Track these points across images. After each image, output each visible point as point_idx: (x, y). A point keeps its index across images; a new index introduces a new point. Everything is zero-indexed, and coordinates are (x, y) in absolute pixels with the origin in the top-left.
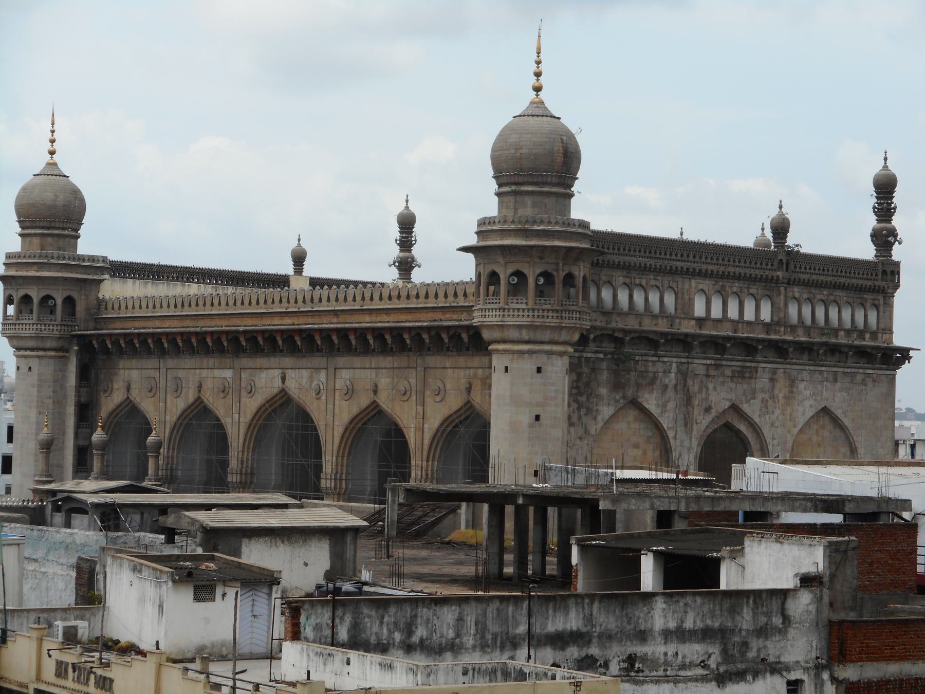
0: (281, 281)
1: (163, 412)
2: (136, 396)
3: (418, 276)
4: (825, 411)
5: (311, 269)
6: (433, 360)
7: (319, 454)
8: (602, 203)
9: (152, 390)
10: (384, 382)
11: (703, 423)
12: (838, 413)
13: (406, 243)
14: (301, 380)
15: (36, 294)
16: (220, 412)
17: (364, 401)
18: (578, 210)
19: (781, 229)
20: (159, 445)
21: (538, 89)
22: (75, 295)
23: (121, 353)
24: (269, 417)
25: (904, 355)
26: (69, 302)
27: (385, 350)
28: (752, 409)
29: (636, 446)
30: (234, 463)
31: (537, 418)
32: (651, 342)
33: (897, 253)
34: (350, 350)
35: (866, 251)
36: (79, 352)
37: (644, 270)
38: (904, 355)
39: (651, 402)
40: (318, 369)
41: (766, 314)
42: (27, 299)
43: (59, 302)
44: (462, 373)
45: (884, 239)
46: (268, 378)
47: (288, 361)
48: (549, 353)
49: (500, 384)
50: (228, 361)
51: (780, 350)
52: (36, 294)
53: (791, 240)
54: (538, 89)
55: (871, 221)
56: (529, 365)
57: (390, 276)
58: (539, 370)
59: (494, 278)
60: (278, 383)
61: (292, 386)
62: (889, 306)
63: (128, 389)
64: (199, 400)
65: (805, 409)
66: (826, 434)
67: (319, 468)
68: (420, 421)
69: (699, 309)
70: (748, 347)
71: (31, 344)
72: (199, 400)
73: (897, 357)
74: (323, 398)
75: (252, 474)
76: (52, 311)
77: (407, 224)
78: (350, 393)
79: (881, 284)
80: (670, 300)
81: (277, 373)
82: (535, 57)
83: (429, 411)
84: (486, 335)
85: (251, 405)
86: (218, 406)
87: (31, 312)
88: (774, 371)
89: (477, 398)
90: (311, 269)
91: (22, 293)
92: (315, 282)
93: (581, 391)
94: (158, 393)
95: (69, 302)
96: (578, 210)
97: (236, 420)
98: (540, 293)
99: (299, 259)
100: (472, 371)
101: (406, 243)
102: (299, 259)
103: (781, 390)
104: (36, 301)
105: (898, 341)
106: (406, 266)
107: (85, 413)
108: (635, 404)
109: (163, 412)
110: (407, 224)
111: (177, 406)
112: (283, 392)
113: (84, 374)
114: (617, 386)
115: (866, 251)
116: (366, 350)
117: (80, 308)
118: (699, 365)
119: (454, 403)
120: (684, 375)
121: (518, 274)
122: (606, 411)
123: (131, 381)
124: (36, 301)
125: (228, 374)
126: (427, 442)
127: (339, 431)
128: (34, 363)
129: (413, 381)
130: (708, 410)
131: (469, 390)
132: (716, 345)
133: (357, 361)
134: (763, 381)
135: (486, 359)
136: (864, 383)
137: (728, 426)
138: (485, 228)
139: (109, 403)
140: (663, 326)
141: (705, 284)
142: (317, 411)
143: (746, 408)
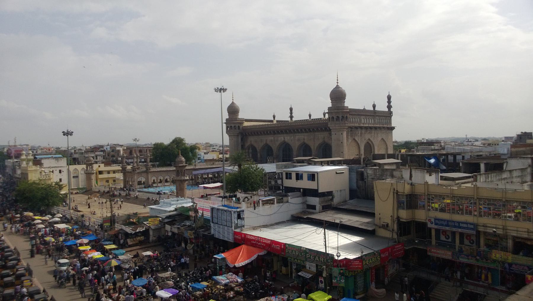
0: (272, 121)
1: (259, 146)
2: (252, 143)
3: (294, 119)
4: (382, 139)
5: (276, 119)
6: (317, 133)
8: (350, 103)
10: (306, 138)
11: (365, 142)
13: (291, 113)
14: (287, 138)
15: (233, 126)
16: (271, 145)
18: (346, 105)
19: (374, 106)
21: (338, 83)
25: (393, 128)
27: (306, 132)
28: (372, 139)
30: (274, 154)
32: (356, 128)
33: (392, 110)
34: (299, 132)
35: (387, 110)
37: (355, 115)
38: (393, 128)
39: (357, 139)
42: (231, 126)
45: (389, 107)
46: (281, 138)
47: (285, 135)
49: (334, 137)
51: (376, 128)
52: (233, 126)
53: (377, 109)
54: (338, 83)
55: (387, 104)
57: (289, 119)
59: (333, 118)
60: (283, 139)
61: (286, 140)
62: (391, 119)
65: (380, 138)
68: (314, 144)
69: (363, 122)
70: (371, 128)
73: (393, 128)
77: (291, 109)
84: (331, 128)
85: (278, 143)
90: (276, 119)
92: (277, 121)
94: (258, 142)
95: (239, 127)
96: (346, 105)
97: (275, 147)
99: (274, 117)
101: (291, 113)
102: (274, 117)
105: (393, 126)
106: (291, 117)
107: (243, 147)
108: (354, 139)
109: (259, 146)
110: (291, 109)
111: (261, 145)
112: (284, 141)
113: (242, 139)
114: (351, 136)
116: (302, 132)
118: (363, 131)
119: (321, 141)
120: (361, 133)
121: (338, 117)
122: (350, 141)
123: (251, 140)
125: (272, 138)
127: (297, 147)
132: (366, 128)
133: (300, 134)
134: (373, 134)
135: (328, 133)
138: (329, 109)
139: (247, 144)
140: (357, 125)
141: (364, 117)
142: (291, 143)
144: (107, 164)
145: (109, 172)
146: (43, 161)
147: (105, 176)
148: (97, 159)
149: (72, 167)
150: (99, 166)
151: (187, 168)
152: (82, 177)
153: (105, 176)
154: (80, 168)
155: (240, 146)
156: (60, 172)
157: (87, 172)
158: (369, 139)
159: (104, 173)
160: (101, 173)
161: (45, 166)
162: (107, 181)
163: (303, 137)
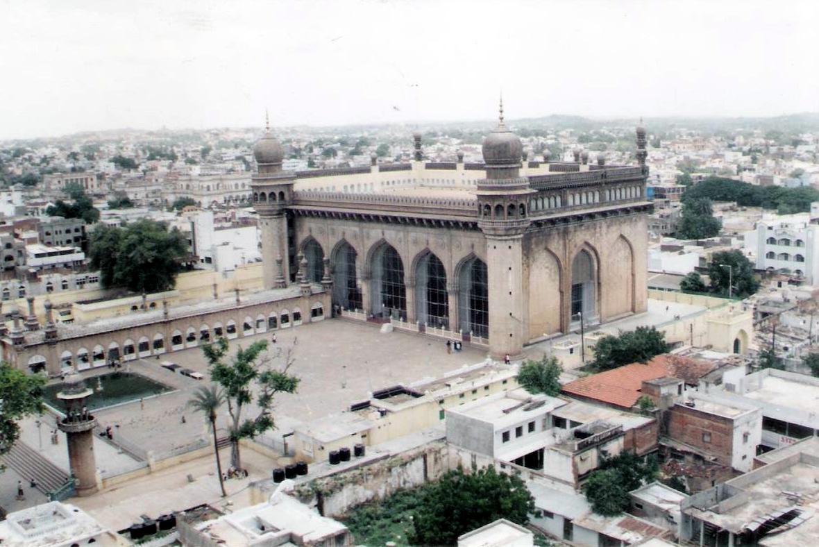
1: (328, 245)
4: (622, 237)
7: (401, 268)
9: (322, 232)
10: (432, 240)
12: (626, 236)
14: (392, 235)
15: (267, 193)
17: (423, 247)
20: (328, 261)
22: (283, 191)
23: (306, 216)
24: (377, 249)
26: (282, 194)
29: (547, 268)
31: (510, 269)
36: (287, 216)
40: (399, 231)
41: (597, 200)
42: (263, 194)
43: (277, 195)
44: (469, 239)
45: (642, 157)
46: (376, 233)
47: (385, 226)
48: (514, 240)
50: (357, 223)
52: (267, 193)
56: (505, 245)
58: (510, 247)
63: (310, 231)
64: (344, 239)
66: (620, 245)
67: (402, 275)
68: (451, 259)
71: (267, 213)
72: (344, 239)
74: (403, 243)
75: (371, 273)
76: (274, 199)
78: (415, 242)
79: (642, 176)
80: (558, 199)
81: (380, 231)
82: (499, 103)
83: (454, 256)
85: (369, 244)
86: (353, 243)
87: (265, 199)
88: (601, 224)
89: (478, 253)
91: (261, 192)
93: (527, 251)
94: (328, 236)
95: (282, 194)
98: (509, 214)
100: (473, 239)
103: (604, 229)
104: (267, 195)
107: (292, 240)
112: (383, 239)
115: (634, 164)
117: (287, 197)
124: (267, 195)
125: (357, 229)
126: (453, 269)
127: (411, 259)
128: (268, 221)
129: (445, 241)
130: (575, 246)
131: (473, 246)
136: (636, 221)
137: (583, 250)
139: (302, 237)
143: (592, 242)
155: (286, 240)
158: (587, 243)
163: (425, 236)
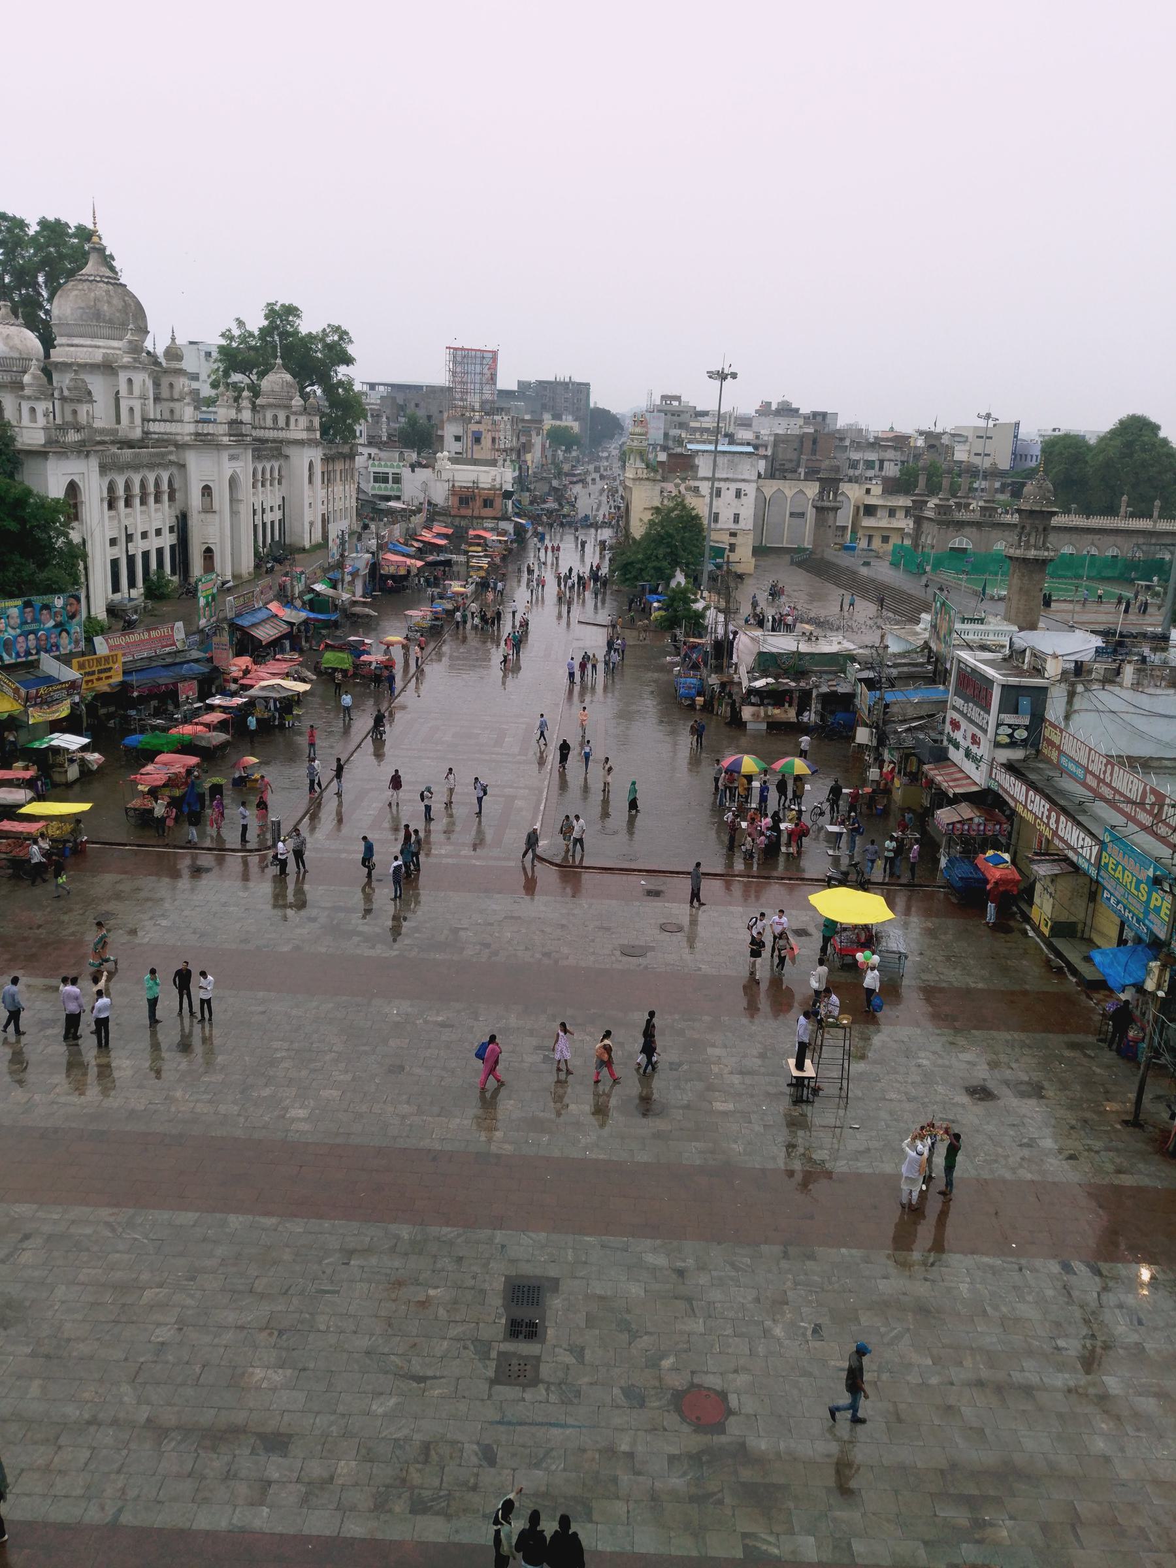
144: (892, 487)
145: (892, 512)
146: (699, 461)
147: (881, 521)
148: (881, 468)
149: (771, 487)
150: (868, 491)
151: (1056, 521)
152: (811, 513)
153: (881, 521)
154: (812, 490)
156: (738, 494)
157: (819, 504)
159: (879, 514)
160: (870, 510)
161: (701, 474)
162: (885, 539)
